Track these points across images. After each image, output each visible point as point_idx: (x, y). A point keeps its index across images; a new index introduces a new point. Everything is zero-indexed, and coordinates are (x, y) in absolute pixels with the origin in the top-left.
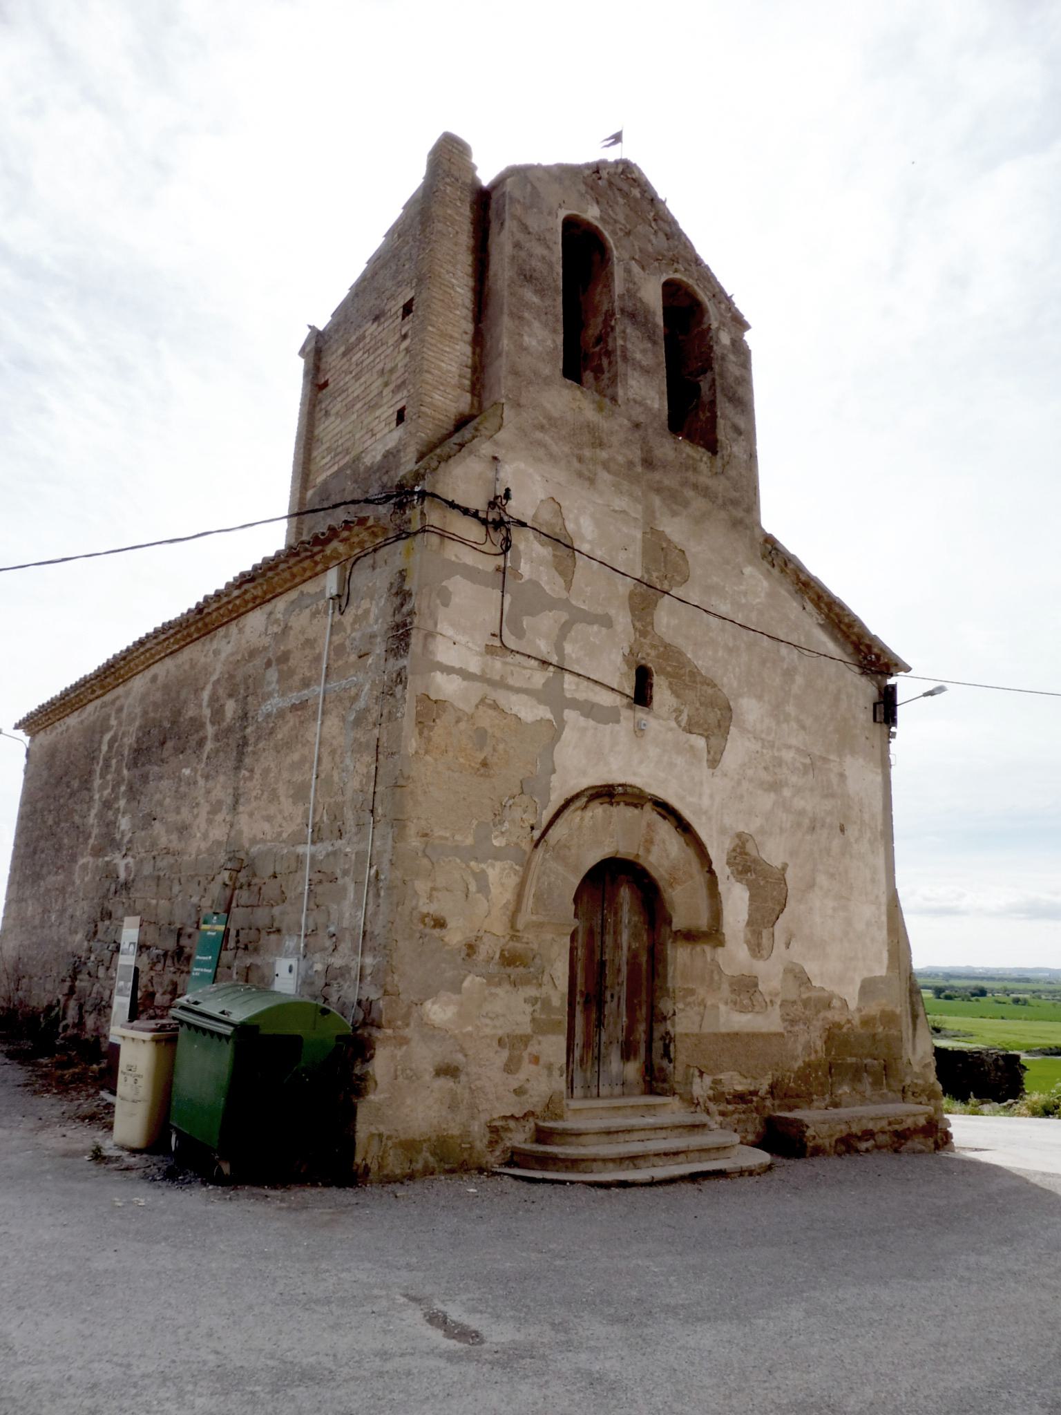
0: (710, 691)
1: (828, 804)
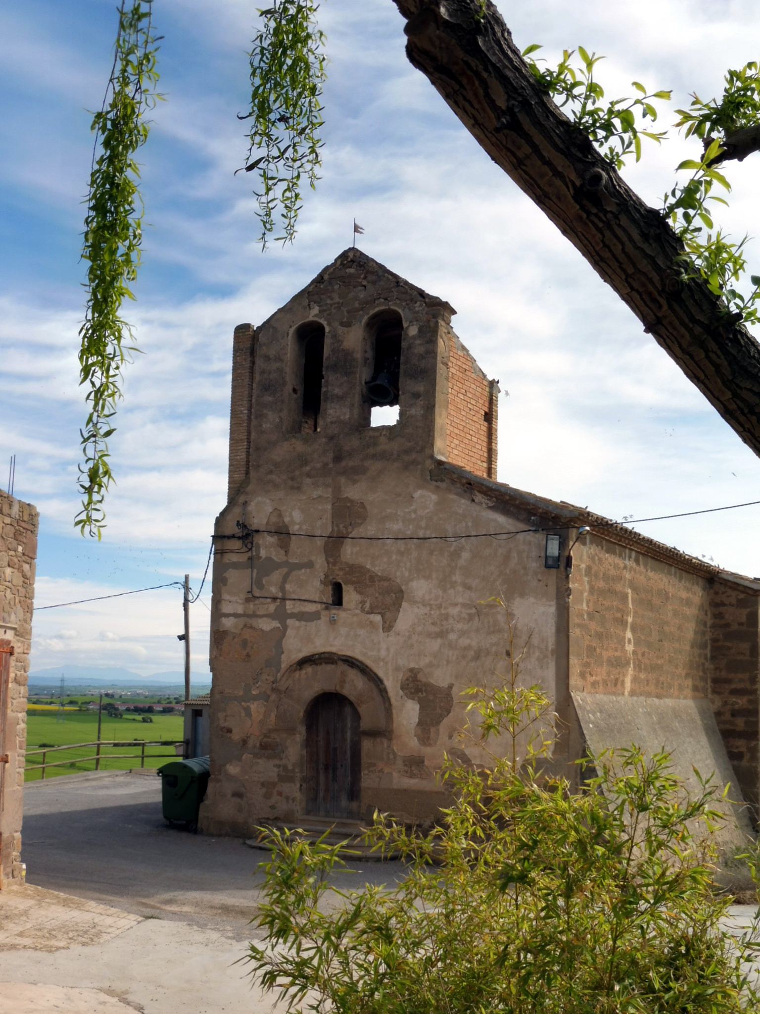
0: (386, 584)
1: (494, 639)
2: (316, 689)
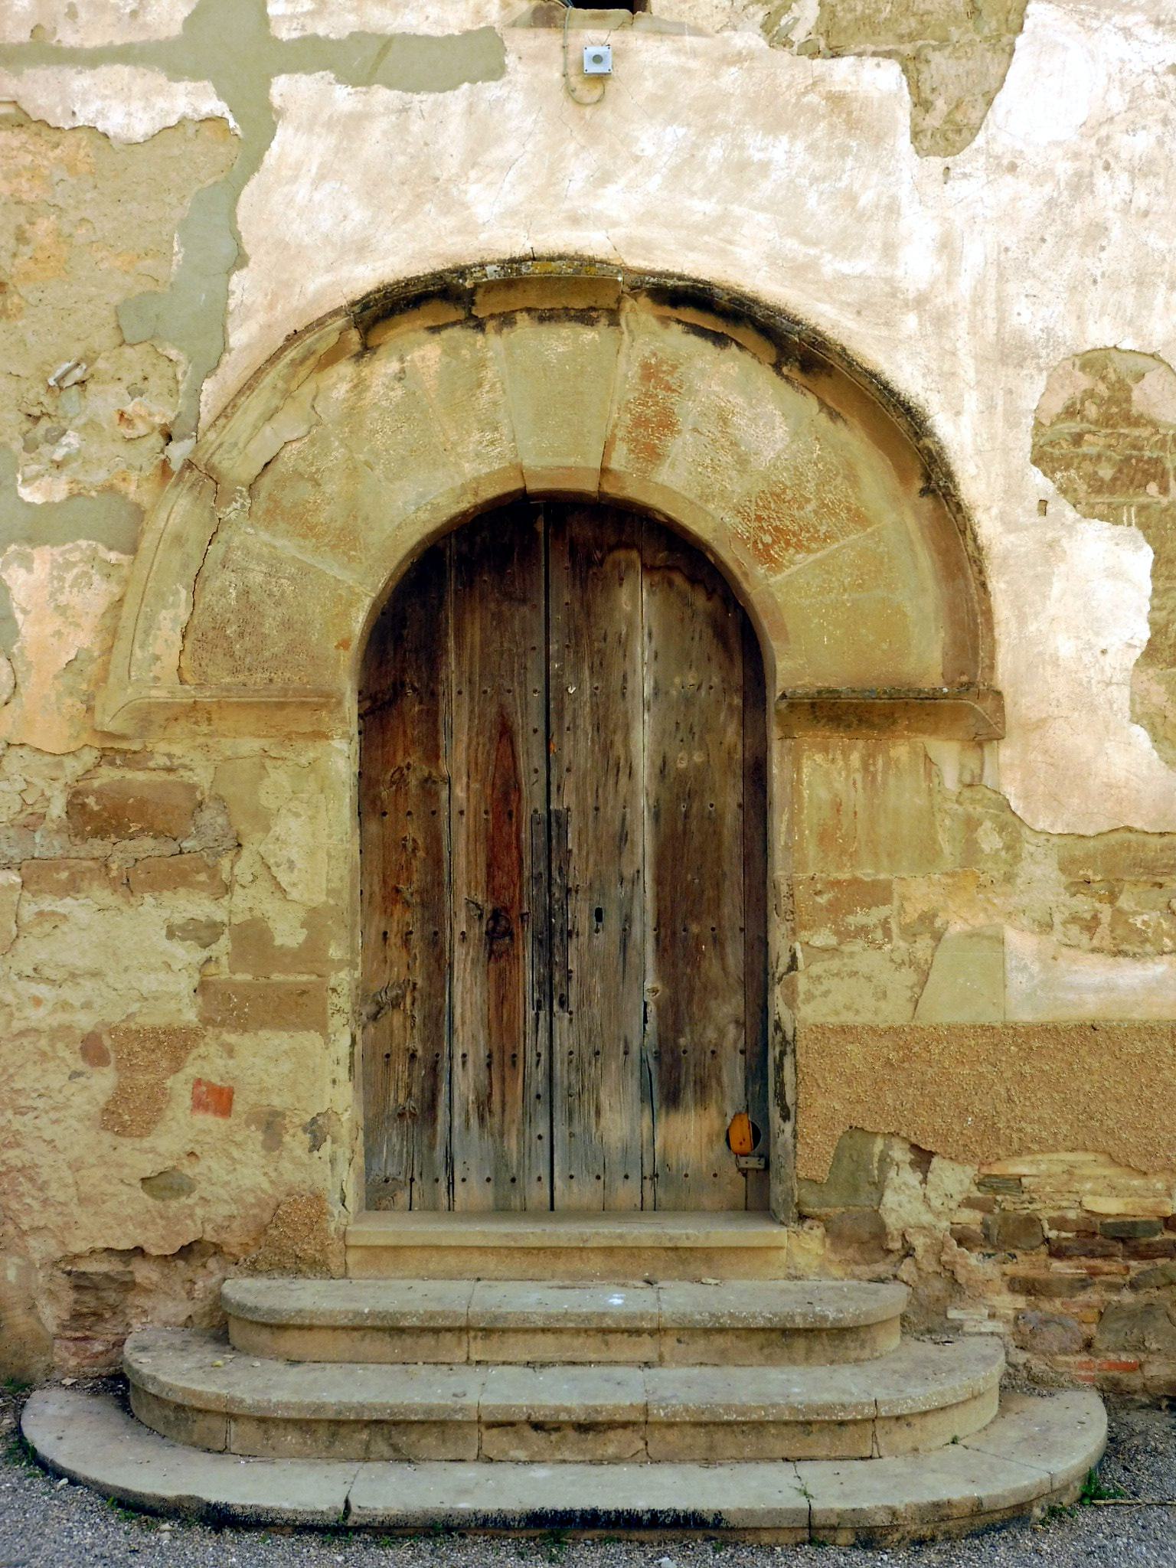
2: (470, 469)
